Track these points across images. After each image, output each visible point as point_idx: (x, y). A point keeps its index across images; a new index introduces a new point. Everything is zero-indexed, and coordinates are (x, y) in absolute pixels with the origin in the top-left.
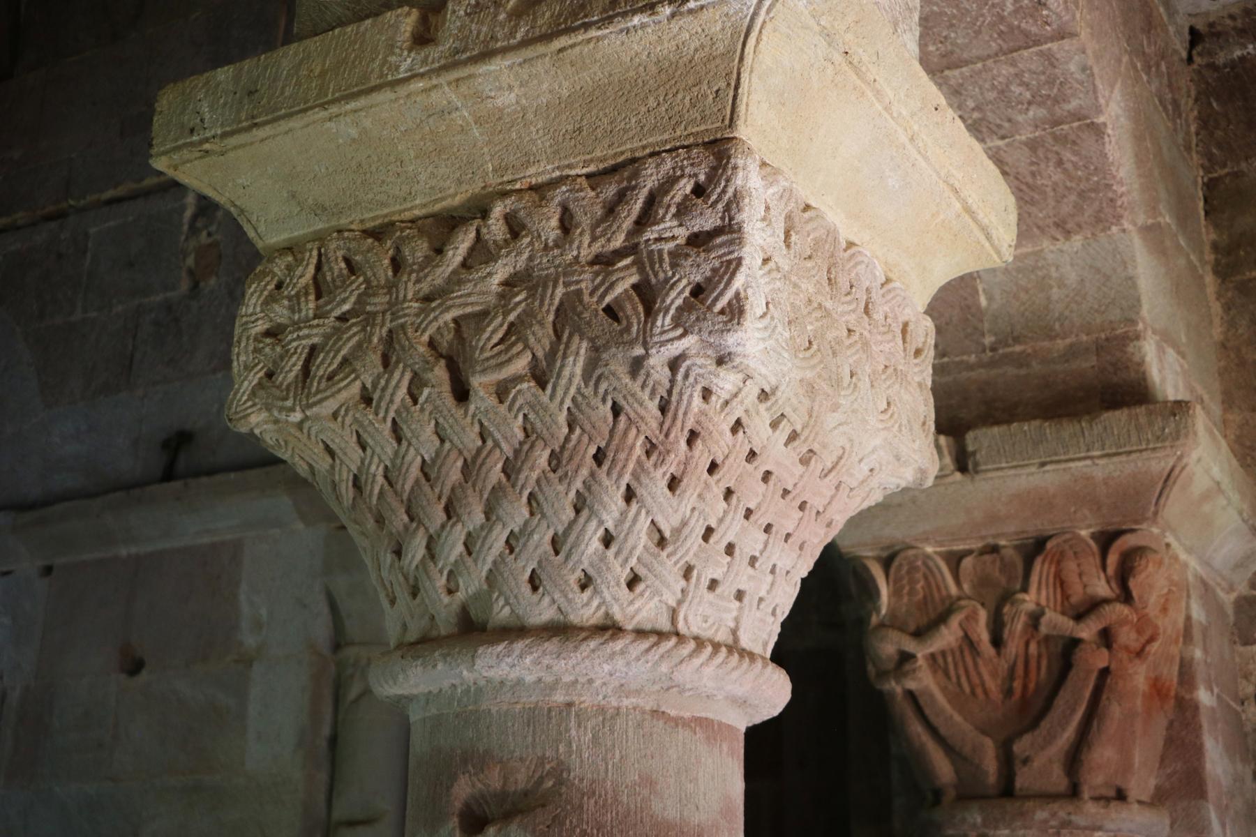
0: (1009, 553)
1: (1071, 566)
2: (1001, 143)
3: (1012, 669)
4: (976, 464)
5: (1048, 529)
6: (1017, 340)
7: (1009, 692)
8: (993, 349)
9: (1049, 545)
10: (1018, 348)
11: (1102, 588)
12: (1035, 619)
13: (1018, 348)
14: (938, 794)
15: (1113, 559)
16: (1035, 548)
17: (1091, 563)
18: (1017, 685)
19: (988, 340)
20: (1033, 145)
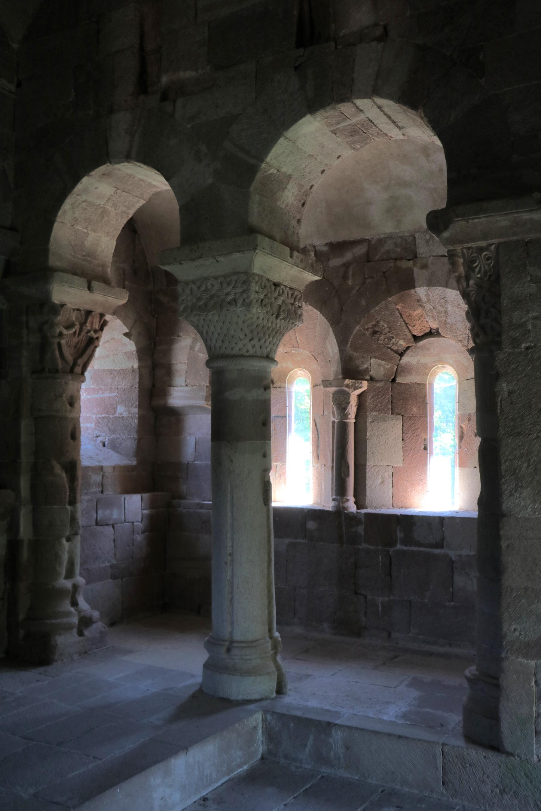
0: (83, 312)
1: (95, 319)
2: (114, 210)
3: (78, 342)
4: (93, 290)
5: (92, 310)
6: (89, 256)
7: (75, 347)
8: (84, 256)
9: (93, 313)
10: (89, 259)
11: (97, 327)
12: (89, 331)
13: (89, 259)
14: (57, 371)
15: (102, 321)
16: (89, 313)
17: (98, 320)
18: (78, 346)
19: (84, 253)
20: (117, 214)
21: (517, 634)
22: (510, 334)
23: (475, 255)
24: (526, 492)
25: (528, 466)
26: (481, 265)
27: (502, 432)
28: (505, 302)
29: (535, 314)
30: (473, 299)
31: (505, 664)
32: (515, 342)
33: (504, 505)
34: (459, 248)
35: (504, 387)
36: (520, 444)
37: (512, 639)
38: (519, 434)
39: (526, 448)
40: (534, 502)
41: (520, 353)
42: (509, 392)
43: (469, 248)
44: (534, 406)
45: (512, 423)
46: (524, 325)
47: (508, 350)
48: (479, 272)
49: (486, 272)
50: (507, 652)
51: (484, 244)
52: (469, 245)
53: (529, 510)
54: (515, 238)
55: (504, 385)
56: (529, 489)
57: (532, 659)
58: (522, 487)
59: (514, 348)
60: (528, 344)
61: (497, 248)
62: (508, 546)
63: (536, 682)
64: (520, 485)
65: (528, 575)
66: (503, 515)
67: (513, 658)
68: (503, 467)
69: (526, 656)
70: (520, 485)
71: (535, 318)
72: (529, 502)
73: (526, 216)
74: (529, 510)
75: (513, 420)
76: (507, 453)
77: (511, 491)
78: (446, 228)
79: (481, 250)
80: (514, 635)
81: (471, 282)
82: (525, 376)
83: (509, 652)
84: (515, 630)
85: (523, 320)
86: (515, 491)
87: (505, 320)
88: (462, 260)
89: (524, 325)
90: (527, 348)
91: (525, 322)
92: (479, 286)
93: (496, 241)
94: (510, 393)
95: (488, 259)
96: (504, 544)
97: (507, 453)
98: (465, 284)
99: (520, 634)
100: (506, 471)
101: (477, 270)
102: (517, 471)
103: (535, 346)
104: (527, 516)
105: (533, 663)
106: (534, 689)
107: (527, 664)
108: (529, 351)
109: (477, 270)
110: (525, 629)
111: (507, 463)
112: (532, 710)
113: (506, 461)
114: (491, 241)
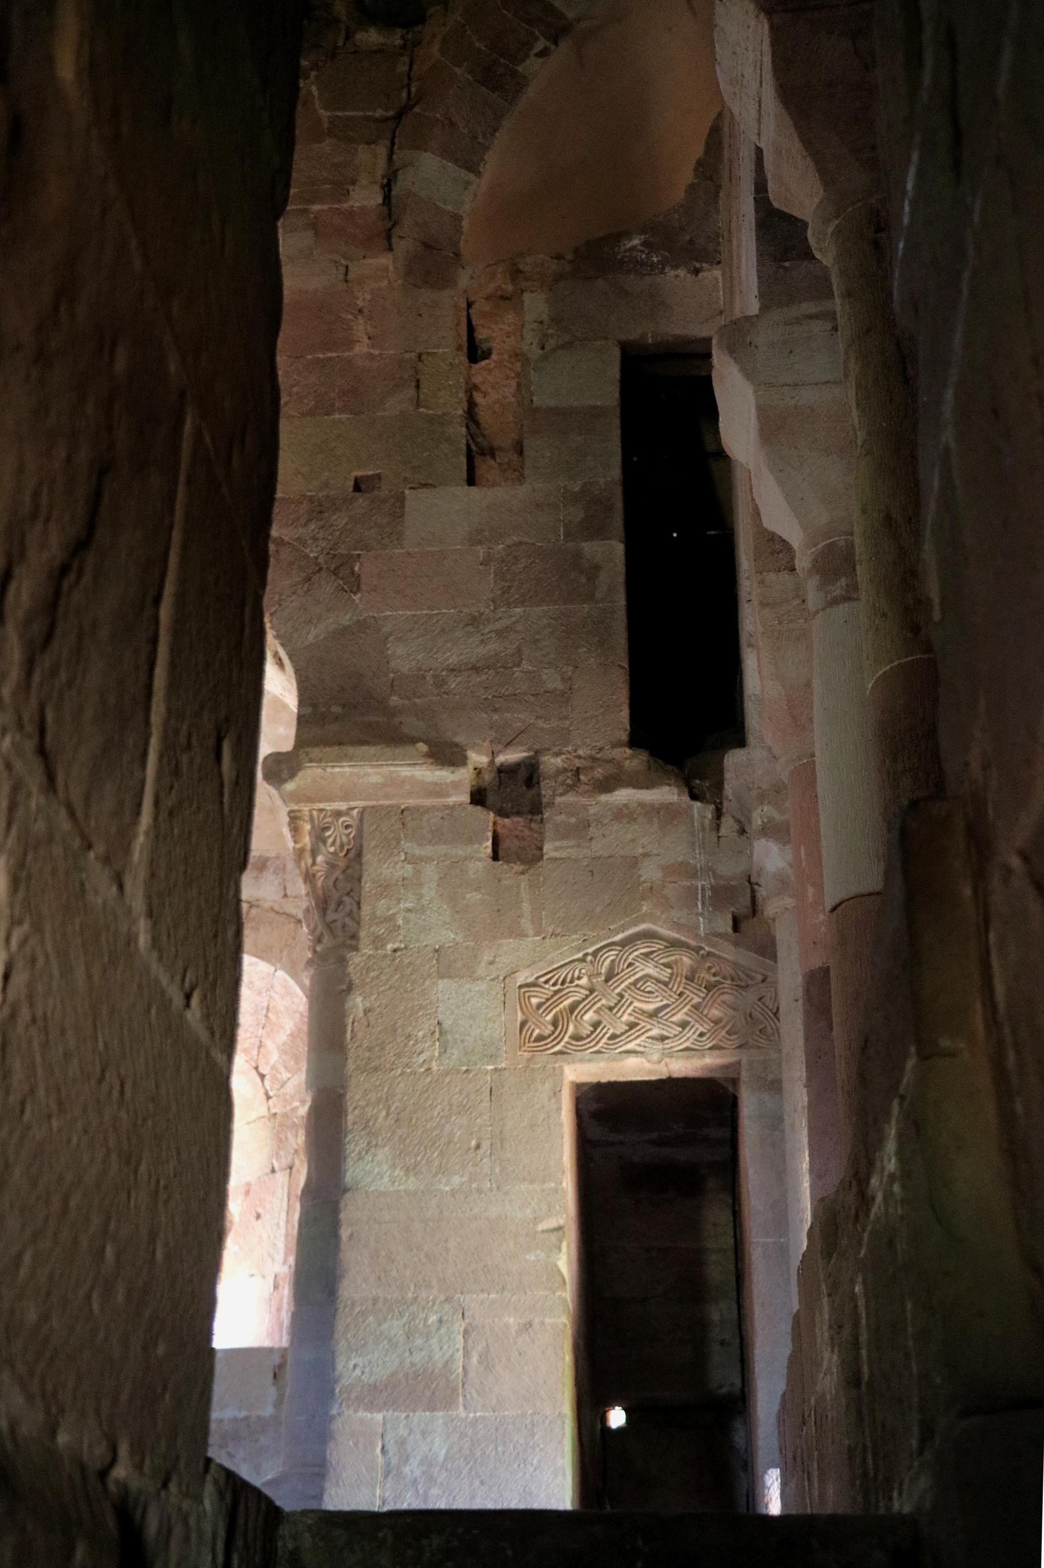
21: (358, 1372)
22: (372, 929)
23: (328, 820)
24: (382, 1154)
25: (388, 1114)
26: (337, 835)
27: (351, 1066)
28: (367, 885)
29: (409, 905)
30: (319, 883)
31: (337, 1425)
32: (378, 942)
33: (348, 1174)
34: (305, 808)
35: (357, 1003)
36: (378, 1083)
37: (350, 1381)
38: (376, 1069)
39: (386, 1090)
40: (394, 1166)
41: (385, 956)
42: (365, 1010)
43: (321, 810)
44: (400, 1030)
45: (367, 1054)
46: (392, 918)
47: (368, 951)
48: (333, 844)
49: (342, 846)
50: (341, 1404)
51: (342, 806)
52: (322, 806)
53: (386, 1179)
54: (387, 802)
55: (359, 1000)
56: (387, 1148)
57: (379, 1411)
58: (376, 1146)
59: (377, 948)
60: (396, 946)
61: (362, 813)
62: (351, 1236)
63: (383, 1448)
64: (374, 1143)
65: (380, 1278)
66: (346, 1190)
67: (351, 1412)
68: (350, 1118)
69: (370, 1407)
70: (374, 1143)
71: (409, 910)
72: (385, 1167)
73: (405, 772)
74: (386, 1179)
75: (370, 1049)
76: (357, 1097)
77: (360, 1153)
78: (292, 775)
79: (338, 814)
80: (354, 1374)
81: (320, 859)
82: (390, 988)
83: (344, 1405)
84: (355, 1366)
85: (391, 912)
86: (367, 1153)
87: (366, 909)
88: (308, 827)
89: (392, 918)
90: (395, 951)
91: (394, 915)
92: (331, 866)
93: (361, 804)
94: (366, 1012)
95: (347, 827)
96: (344, 1233)
97: (357, 1097)
98: (310, 861)
99: (363, 1373)
100: (354, 1124)
101: (330, 841)
102: (371, 1123)
103: (406, 948)
104: (382, 1189)
105: (379, 1417)
106: (380, 1460)
107: (372, 1419)
108: (399, 953)
109: (330, 841)
110: (370, 1362)
111: (357, 1112)
112: (374, 1495)
113: (355, 1108)
114: (353, 804)
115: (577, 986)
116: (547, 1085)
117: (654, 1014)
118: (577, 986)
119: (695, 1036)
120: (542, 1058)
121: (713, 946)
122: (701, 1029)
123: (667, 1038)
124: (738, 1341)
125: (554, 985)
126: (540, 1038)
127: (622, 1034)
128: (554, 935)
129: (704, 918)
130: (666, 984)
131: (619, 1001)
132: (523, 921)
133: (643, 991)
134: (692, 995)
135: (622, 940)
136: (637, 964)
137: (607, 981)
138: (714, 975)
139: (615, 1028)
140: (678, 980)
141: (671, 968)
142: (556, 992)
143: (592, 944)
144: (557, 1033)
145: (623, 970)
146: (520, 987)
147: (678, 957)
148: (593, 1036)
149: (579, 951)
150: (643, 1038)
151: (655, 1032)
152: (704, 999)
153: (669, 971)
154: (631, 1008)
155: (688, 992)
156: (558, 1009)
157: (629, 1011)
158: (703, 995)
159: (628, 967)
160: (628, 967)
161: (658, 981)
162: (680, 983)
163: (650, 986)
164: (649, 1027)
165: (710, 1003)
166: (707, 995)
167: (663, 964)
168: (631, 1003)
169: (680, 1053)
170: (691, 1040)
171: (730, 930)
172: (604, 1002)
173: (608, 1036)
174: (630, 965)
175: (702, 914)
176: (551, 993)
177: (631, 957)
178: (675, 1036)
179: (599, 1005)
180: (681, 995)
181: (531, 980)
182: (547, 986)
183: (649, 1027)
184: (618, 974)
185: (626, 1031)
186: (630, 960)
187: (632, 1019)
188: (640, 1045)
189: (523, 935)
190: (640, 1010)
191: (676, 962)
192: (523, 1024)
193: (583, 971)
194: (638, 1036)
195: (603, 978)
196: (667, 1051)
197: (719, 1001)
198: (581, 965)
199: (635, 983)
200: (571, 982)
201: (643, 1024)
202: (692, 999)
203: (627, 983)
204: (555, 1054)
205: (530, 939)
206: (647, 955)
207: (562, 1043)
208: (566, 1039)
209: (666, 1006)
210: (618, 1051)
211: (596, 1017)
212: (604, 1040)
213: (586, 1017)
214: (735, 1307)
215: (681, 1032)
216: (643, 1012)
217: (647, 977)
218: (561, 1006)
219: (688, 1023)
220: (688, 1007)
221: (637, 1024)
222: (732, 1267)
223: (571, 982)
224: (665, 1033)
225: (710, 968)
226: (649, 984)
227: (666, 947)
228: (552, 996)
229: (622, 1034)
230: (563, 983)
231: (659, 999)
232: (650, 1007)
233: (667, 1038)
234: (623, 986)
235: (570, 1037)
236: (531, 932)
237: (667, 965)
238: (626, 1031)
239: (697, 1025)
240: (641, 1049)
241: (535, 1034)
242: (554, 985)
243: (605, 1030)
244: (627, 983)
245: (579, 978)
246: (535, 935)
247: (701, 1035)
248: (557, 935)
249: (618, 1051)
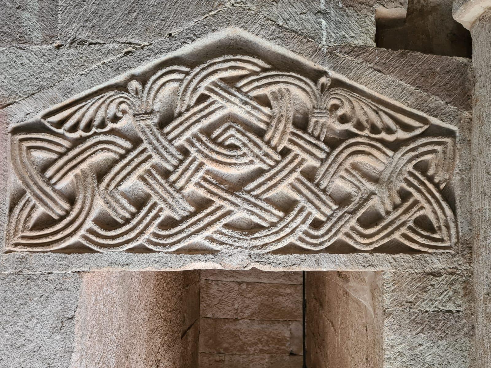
115: (112, 132)
116: (49, 307)
117: (236, 187)
118: (112, 132)
119: (305, 227)
120: (41, 261)
121: (341, 70)
122: (316, 215)
123: (260, 228)
124: (302, 353)
125: (74, 128)
126: (46, 222)
127: (184, 219)
128: (76, 42)
129: (329, 21)
130: (260, 133)
131: (181, 162)
132: (25, 15)
133: (221, 145)
134: (303, 155)
135: (192, 55)
136: (214, 97)
137: (162, 125)
138: (343, 119)
139: (171, 207)
140: (281, 127)
141: (268, 104)
142: (77, 142)
143: (140, 61)
144: (73, 214)
145: (187, 110)
146: (15, 131)
147: (282, 86)
148: (134, 222)
149: (117, 70)
150: (218, 226)
151: (240, 215)
152: (323, 161)
153: (267, 110)
154: (201, 173)
155: (296, 150)
156: (77, 171)
157: (197, 178)
158: (322, 156)
159: (198, 102)
160: (198, 102)
161: (249, 127)
162: (284, 132)
163: (234, 137)
164: (228, 207)
165: (332, 170)
166: (328, 154)
167: (257, 99)
168: (201, 165)
169: (278, 256)
170: (299, 233)
171: (372, 43)
172: (156, 159)
173: (159, 220)
174: (203, 98)
175: (325, 14)
176: (67, 144)
177: (207, 83)
178: (273, 225)
179: (147, 166)
180: (285, 152)
181: (38, 117)
182: (61, 131)
183: (228, 207)
184: (180, 114)
185: (192, 215)
186: (202, 90)
187: (202, 193)
188: (211, 239)
189: (23, 40)
190: (215, 176)
191: (278, 96)
192: (18, 196)
193: (123, 106)
194: (210, 224)
195: (156, 120)
196: (256, 251)
197: (347, 165)
198: (119, 96)
199: (208, 131)
200: (103, 125)
201: (218, 202)
202: (303, 160)
203: (195, 129)
204: (68, 250)
205: (36, 48)
206: (231, 82)
207: (82, 232)
208: (89, 224)
209: (260, 172)
210: (174, 248)
211: (143, 188)
212: (153, 228)
213: (124, 187)
214: (301, 327)
215: (281, 219)
216: (220, 181)
217: (232, 119)
218: (84, 166)
219: (294, 203)
220: (296, 175)
221: (209, 202)
222: (301, 299)
223: (103, 125)
224: (256, 220)
225: (335, 107)
226: (232, 132)
227: (264, 70)
228: (69, 150)
229: (184, 219)
230: (88, 127)
231: (246, 160)
232: (234, 173)
233: (260, 228)
234: (188, 134)
235: (96, 221)
236: (37, 36)
237: (264, 101)
238: (192, 215)
239: (310, 208)
240: (214, 246)
241: (36, 216)
242: (74, 128)
243: (155, 211)
244: (195, 129)
245: (115, 119)
246: (45, 42)
247: (317, 224)
248: (82, 43)
249: (174, 248)
